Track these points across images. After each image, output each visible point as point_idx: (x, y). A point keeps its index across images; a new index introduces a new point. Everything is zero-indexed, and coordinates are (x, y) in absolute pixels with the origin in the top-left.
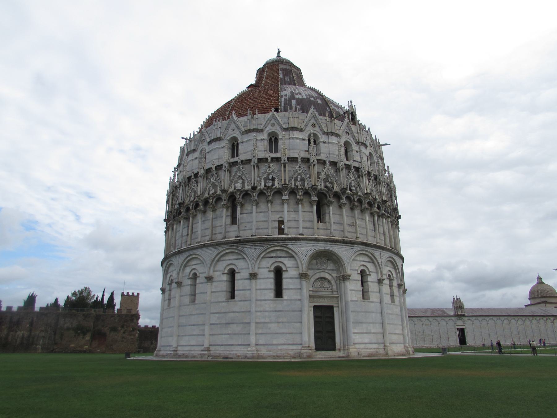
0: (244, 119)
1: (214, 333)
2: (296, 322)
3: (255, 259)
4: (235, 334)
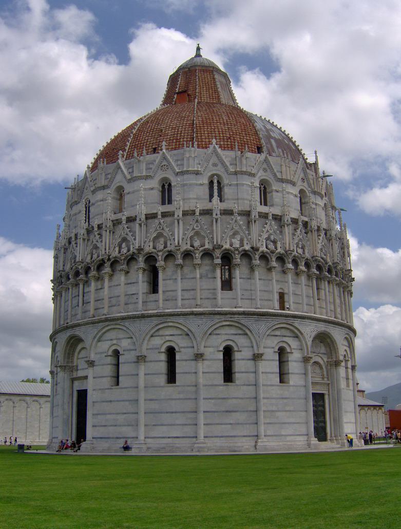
0: (231, 154)
1: (208, 421)
2: (301, 411)
4: (238, 424)
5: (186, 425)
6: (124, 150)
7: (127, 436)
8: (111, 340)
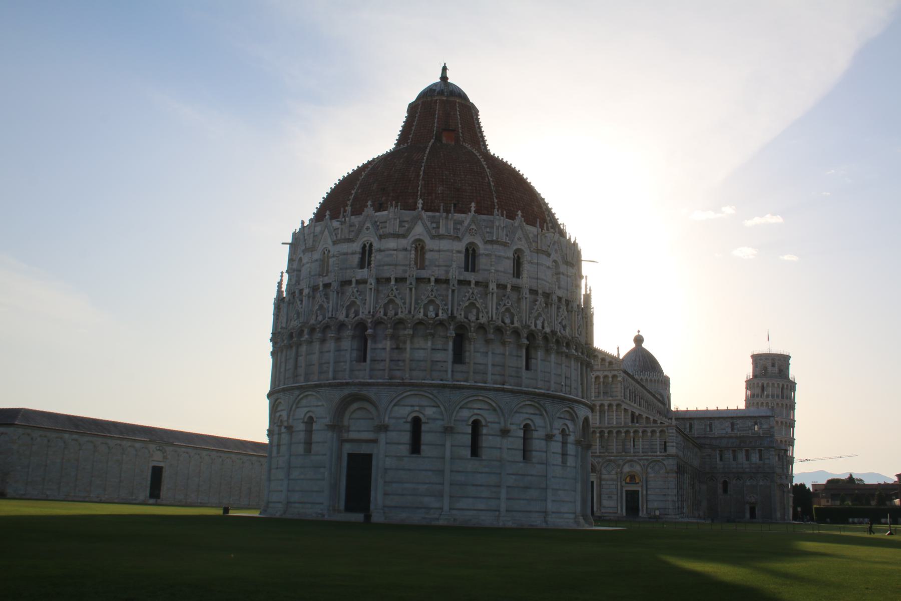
8: (412, 406)
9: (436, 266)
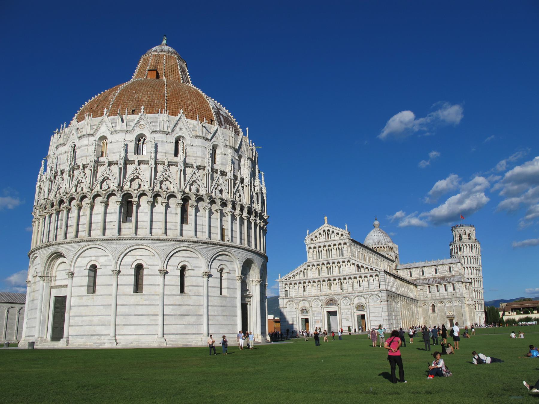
3: (209, 260)
4: (190, 324)
5: (149, 325)
6: (107, 108)
7: (101, 334)
8: (90, 257)
9: (113, 153)
